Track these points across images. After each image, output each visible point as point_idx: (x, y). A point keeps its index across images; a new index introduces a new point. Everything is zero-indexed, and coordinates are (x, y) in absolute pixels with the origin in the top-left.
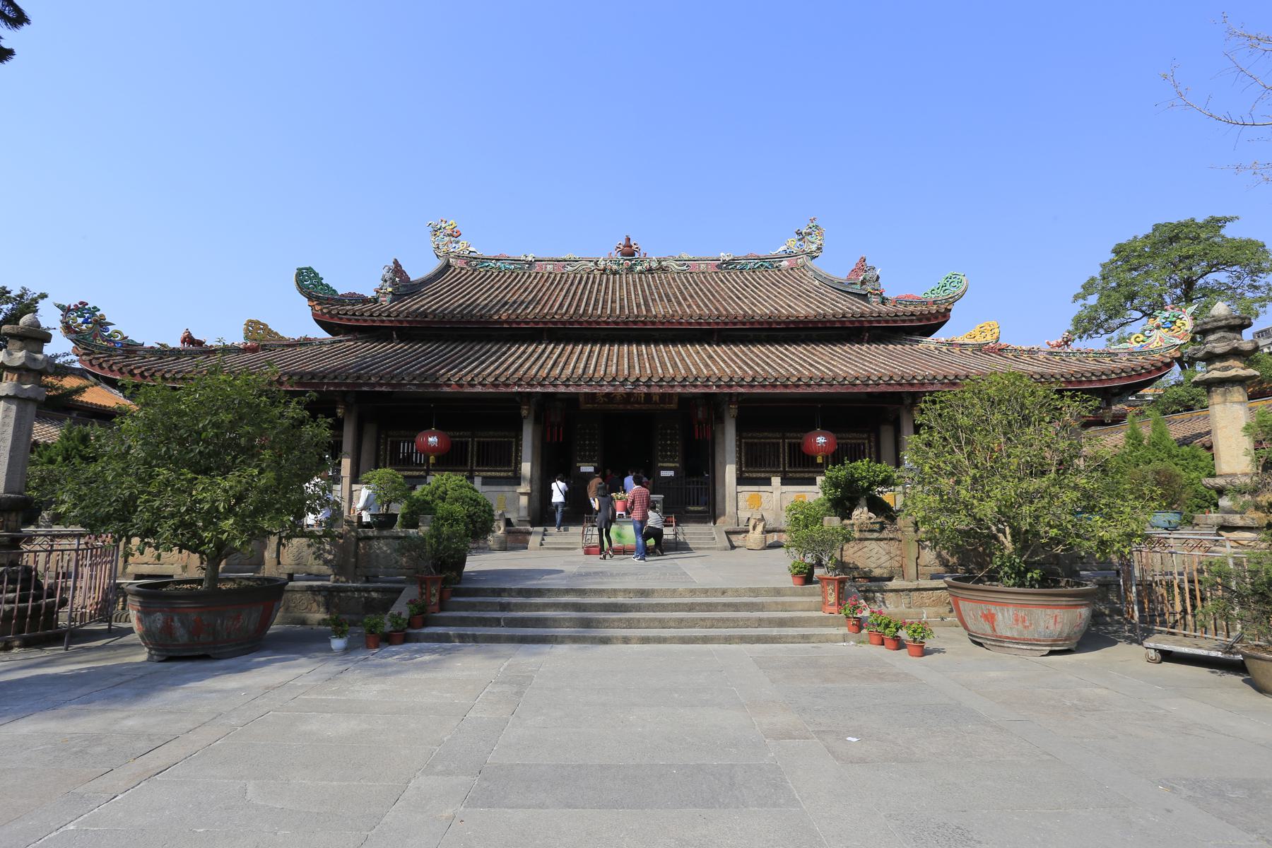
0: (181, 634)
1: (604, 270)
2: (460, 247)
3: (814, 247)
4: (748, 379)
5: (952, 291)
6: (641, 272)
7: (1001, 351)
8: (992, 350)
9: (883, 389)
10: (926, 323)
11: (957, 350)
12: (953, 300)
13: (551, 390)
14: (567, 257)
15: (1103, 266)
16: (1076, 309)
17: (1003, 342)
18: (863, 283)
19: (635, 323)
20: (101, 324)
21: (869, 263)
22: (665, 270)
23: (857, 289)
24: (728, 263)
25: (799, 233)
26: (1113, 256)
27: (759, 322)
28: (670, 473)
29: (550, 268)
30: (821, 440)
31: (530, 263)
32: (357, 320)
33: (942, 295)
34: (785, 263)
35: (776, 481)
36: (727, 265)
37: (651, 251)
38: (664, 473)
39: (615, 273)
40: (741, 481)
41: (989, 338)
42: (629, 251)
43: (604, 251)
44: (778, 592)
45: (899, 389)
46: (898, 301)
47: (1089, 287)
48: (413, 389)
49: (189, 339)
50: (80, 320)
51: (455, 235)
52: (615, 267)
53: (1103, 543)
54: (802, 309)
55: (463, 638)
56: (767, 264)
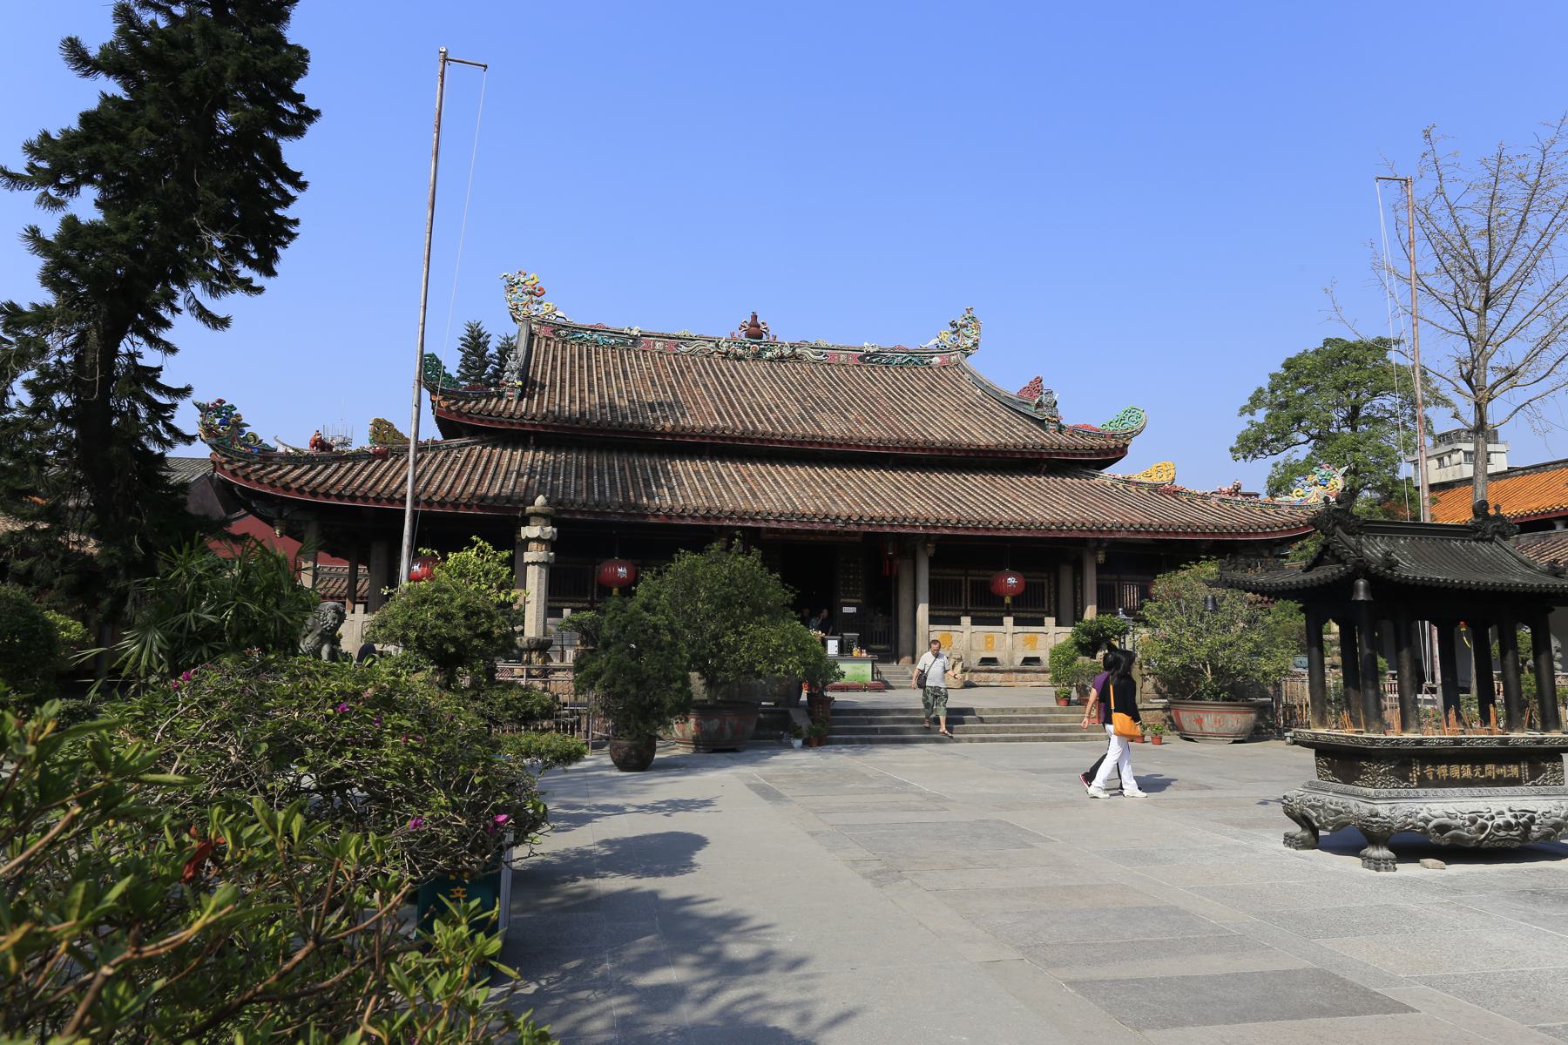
0: (728, 732)
1: (727, 353)
2: (544, 310)
3: (969, 343)
4: (954, 521)
5: (1130, 425)
6: (771, 360)
7: (1176, 493)
8: (1168, 492)
9: (1075, 534)
11: (1132, 489)
12: (1130, 435)
13: (763, 525)
14: (681, 333)
15: (1272, 376)
16: (1242, 425)
17: (1179, 484)
18: (1039, 405)
19: (810, 443)
20: (238, 425)
21: (1046, 385)
22: (797, 358)
23: (1031, 411)
24: (873, 355)
25: (953, 324)
26: (1281, 371)
27: (939, 449)
28: (852, 610)
29: (659, 346)
30: (1011, 580)
31: (635, 338)
32: (491, 422)
33: (1120, 429)
34: (936, 360)
35: (966, 620)
37: (784, 331)
38: (846, 610)
39: (739, 358)
40: (933, 620)
41: (1165, 479)
42: (755, 331)
43: (725, 327)
44: (1051, 710)
45: (1090, 535)
46: (1075, 431)
47: (1256, 401)
48: (618, 518)
49: (320, 444)
50: (218, 421)
51: (536, 293)
52: (740, 351)
53: (1265, 674)
54: (981, 434)
55: (863, 742)
56: (916, 360)
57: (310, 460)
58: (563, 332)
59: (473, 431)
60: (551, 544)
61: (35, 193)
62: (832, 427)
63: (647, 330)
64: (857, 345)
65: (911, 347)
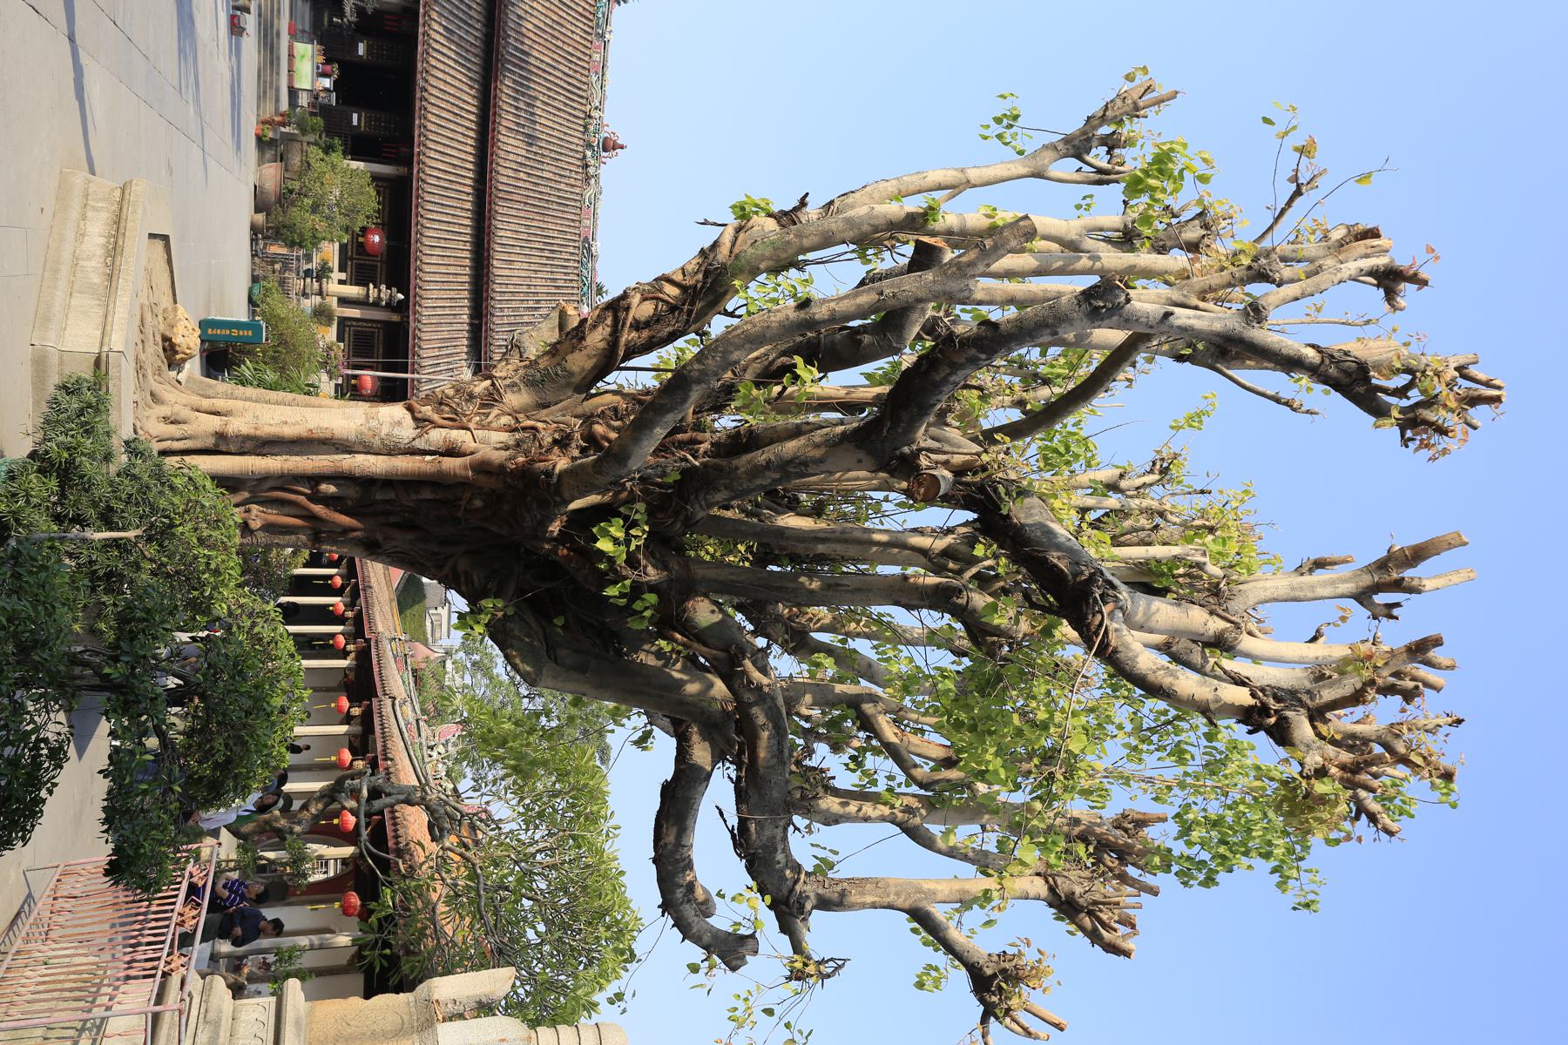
13: (421, 21)
14: (608, 76)
22: (588, 179)
24: (589, 250)
28: (355, 122)
29: (596, 57)
30: (377, 239)
31: (602, 36)
37: (610, 170)
38: (355, 116)
42: (610, 146)
43: (614, 118)
52: (591, 128)
62: (509, 145)
63: (610, 47)
64: (598, 236)
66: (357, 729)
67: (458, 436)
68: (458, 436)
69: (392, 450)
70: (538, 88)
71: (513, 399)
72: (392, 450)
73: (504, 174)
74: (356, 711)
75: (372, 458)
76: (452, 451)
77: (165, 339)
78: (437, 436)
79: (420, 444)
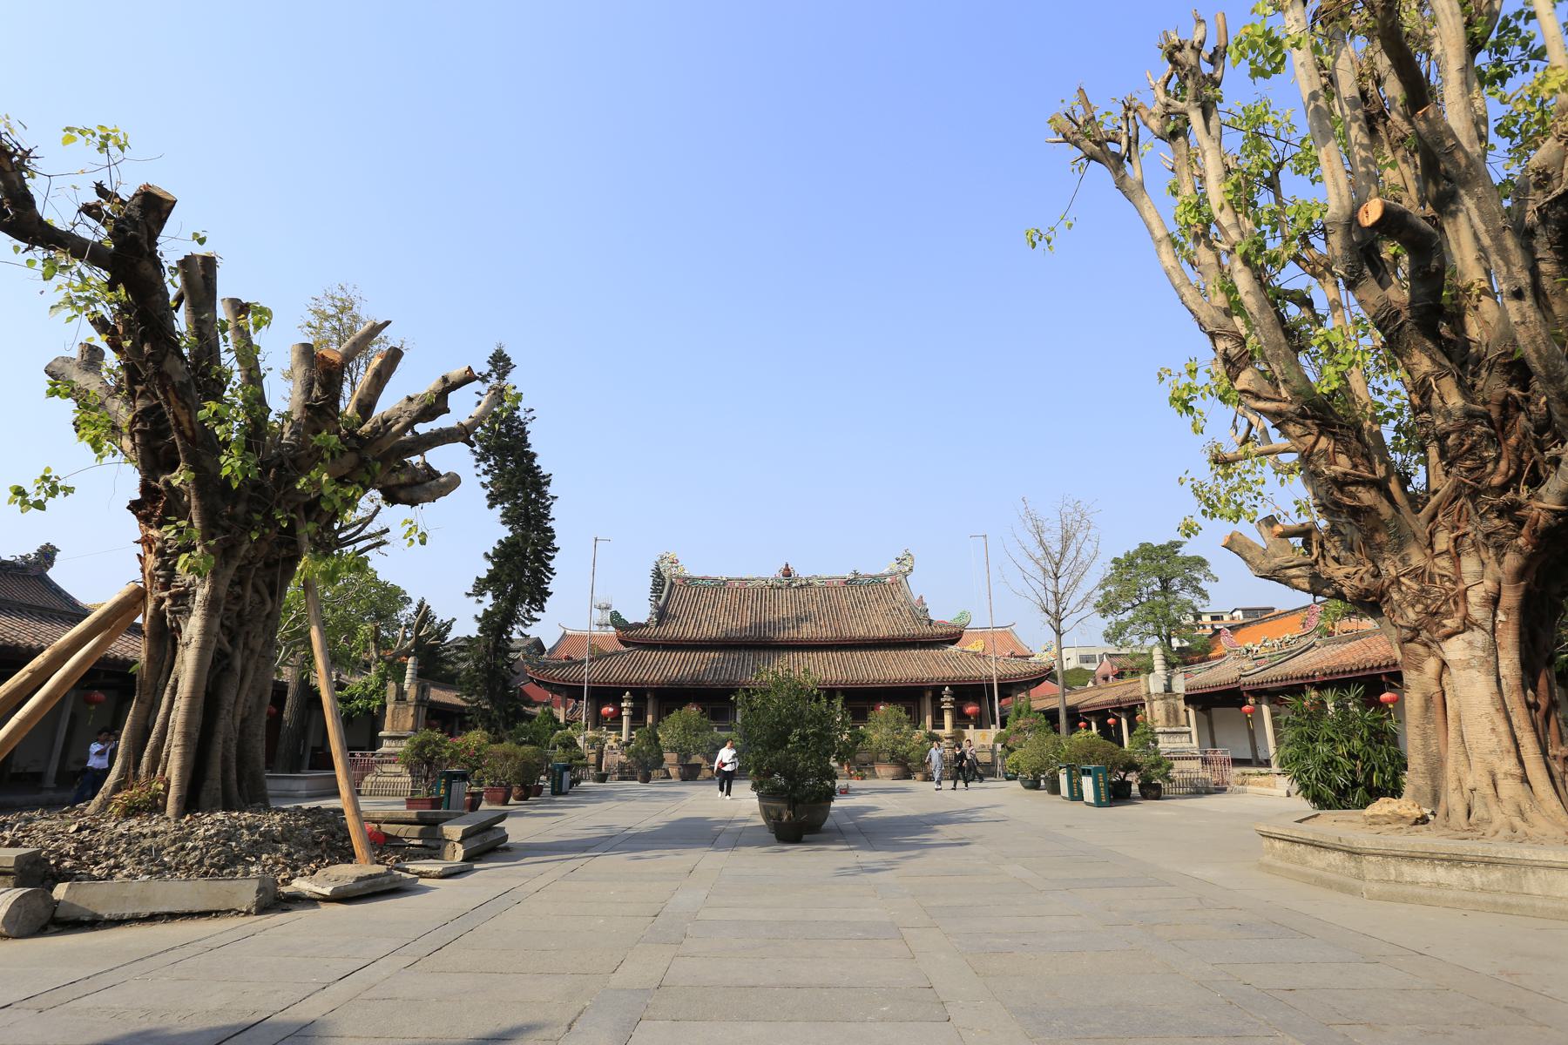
10: (953, 638)
22: (809, 584)
33: (958, 622)
36: (852, 582)
37: (802, 571)
42: (787, 573)
43: (772, 572)
49: (568, 658)
56: (877, 581)
57: (564, 666)
58: (689, 582)
59: (635, 644)
60: (631, 709)
61: (474, 599)
62: (807, 631)
65: (873, 574)
66: (1264, 698)
67: (1475, 596)
68: (1475, 596)
69: (1494, 648)
70: (769, 616)
71: (1417, 558)
72: (1494, 648)
73: (825, 633)
74: (1251, 700)
75: (1503, 663)
76: (1494, 601)
77: (1416, 823)
78: (1478, 613)
79: (1488, 626)
